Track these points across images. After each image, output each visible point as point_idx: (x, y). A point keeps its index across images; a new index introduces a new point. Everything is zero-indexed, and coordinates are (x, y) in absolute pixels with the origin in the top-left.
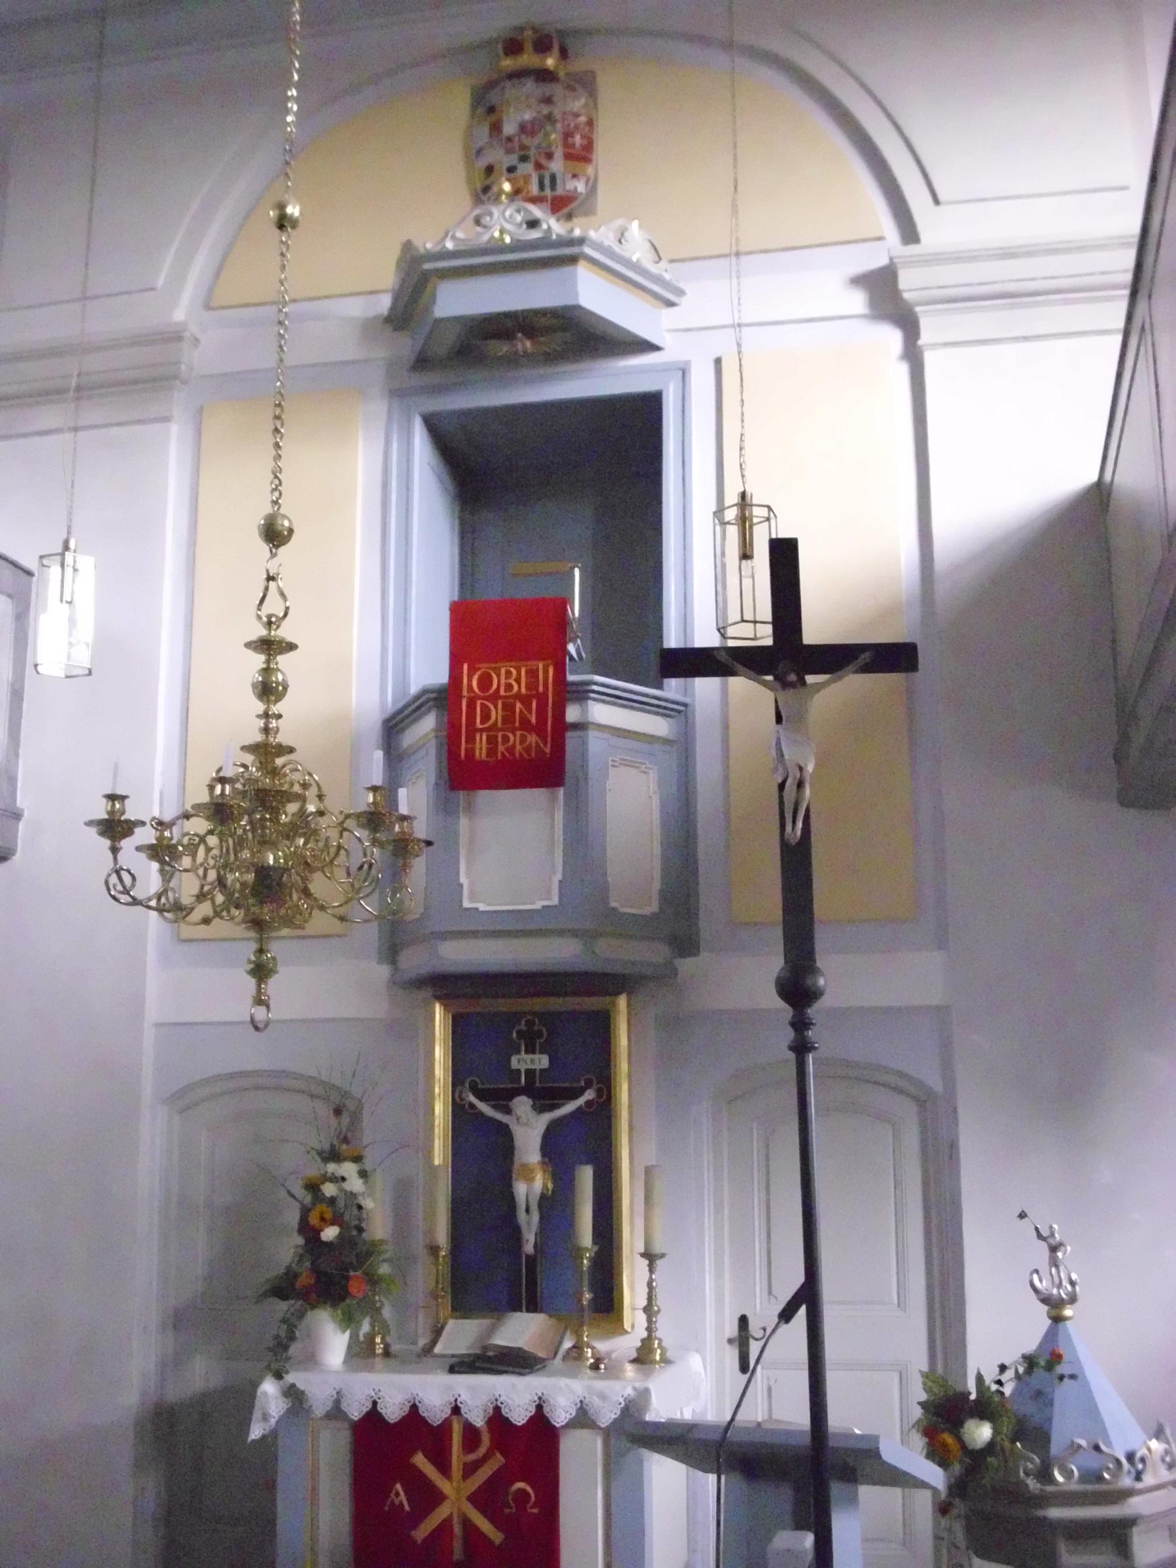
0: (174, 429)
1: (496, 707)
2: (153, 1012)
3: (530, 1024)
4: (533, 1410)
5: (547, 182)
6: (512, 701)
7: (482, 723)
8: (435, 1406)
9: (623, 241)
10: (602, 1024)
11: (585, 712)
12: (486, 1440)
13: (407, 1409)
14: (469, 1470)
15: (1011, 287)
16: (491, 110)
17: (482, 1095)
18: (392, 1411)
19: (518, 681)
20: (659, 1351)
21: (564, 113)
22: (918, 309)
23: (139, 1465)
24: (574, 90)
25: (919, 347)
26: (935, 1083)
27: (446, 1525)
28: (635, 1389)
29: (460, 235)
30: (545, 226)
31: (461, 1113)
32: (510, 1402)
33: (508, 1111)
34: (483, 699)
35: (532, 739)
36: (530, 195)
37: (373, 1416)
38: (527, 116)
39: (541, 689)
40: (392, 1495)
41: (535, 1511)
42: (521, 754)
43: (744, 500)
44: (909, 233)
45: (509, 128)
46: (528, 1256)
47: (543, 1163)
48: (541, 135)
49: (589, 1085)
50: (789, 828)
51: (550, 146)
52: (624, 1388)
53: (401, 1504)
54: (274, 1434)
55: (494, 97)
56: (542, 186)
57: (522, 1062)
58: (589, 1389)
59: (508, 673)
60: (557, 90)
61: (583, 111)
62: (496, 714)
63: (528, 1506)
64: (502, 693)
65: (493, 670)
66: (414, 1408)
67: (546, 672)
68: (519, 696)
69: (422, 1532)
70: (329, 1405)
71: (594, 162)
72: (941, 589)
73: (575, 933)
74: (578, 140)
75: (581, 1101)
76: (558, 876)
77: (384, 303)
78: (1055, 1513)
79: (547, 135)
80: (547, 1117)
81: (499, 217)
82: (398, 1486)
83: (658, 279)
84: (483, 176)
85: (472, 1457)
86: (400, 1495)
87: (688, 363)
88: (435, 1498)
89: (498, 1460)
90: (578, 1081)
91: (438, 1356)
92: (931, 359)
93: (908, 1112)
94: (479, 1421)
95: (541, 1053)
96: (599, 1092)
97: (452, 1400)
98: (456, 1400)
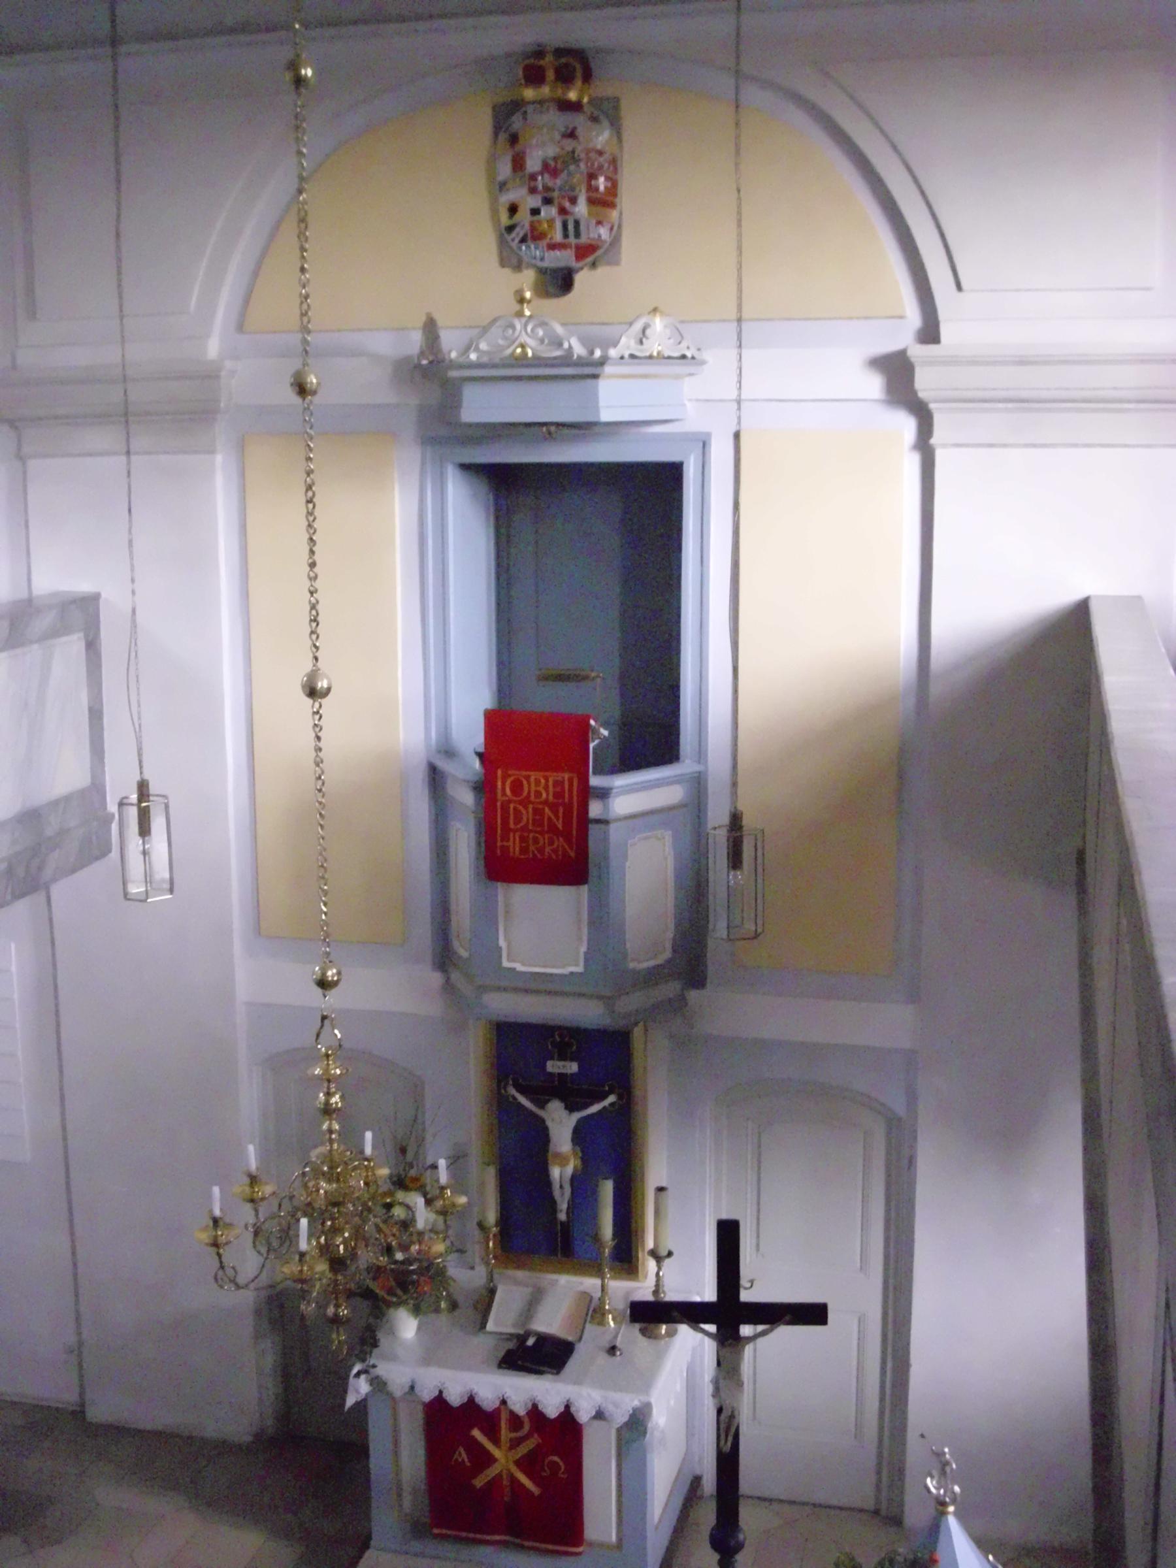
0: (219, 458)
4: (562, 1409)
5: (571, 227)
6: (540, 806)
7: (516, 824)
8: (488, 1398)
9: (644, 340)
11: (606, 808)
12: (527, 1427)
13: (466, 1400)
14: (515, 1444)
15: (1024, 394)
16: (514, 139)
17: (522, 1090)
18: (455, 1397)
19: (546, 788)
22: (932, 406)
23: (258, 1336)
27: (496, 1481)
28: (640, 1400)
29: (483, 346)
30: (566, 345)
34: (515, 802)
35: (560, 842)
36: (553, 241)
38: (551, 151)
39: (567, 795)
43: (736, 821)
45: (533, 164)
46: (562, 1223)
48: (564, 175)
50: (722, 1442)
51: (573, 189)
53: (463, 1461)
54: (365, 1400)
55: (516, 122)
56: (566, 236)
57: (554, 1066)
59: (538, 782)
60: (579, 121)
62: (527, 815)
63: (561, 1472)
64: (532, 798)
65: (520, 804)
68: (546, 802)
69: (479, 1482)
70: (407, 1389)
71: (618, 207)
72: (936, 690)
73: (600, 997)
74: (601, 183)
76: (583, 949)
79: (570, 174)
80: (577, 1116)
81: (521, 331)
82: (462, 1450)
85: (513, 1435)
86: (462, 1455)
87: (709, 435)
88: (490, 1460)
90: (604, 1086)
91: (491, 1333)
92: (941, 457)
94: (520, 1409)
96: (620, 1097)
97: (501, 1395)
98: (503, 1396)
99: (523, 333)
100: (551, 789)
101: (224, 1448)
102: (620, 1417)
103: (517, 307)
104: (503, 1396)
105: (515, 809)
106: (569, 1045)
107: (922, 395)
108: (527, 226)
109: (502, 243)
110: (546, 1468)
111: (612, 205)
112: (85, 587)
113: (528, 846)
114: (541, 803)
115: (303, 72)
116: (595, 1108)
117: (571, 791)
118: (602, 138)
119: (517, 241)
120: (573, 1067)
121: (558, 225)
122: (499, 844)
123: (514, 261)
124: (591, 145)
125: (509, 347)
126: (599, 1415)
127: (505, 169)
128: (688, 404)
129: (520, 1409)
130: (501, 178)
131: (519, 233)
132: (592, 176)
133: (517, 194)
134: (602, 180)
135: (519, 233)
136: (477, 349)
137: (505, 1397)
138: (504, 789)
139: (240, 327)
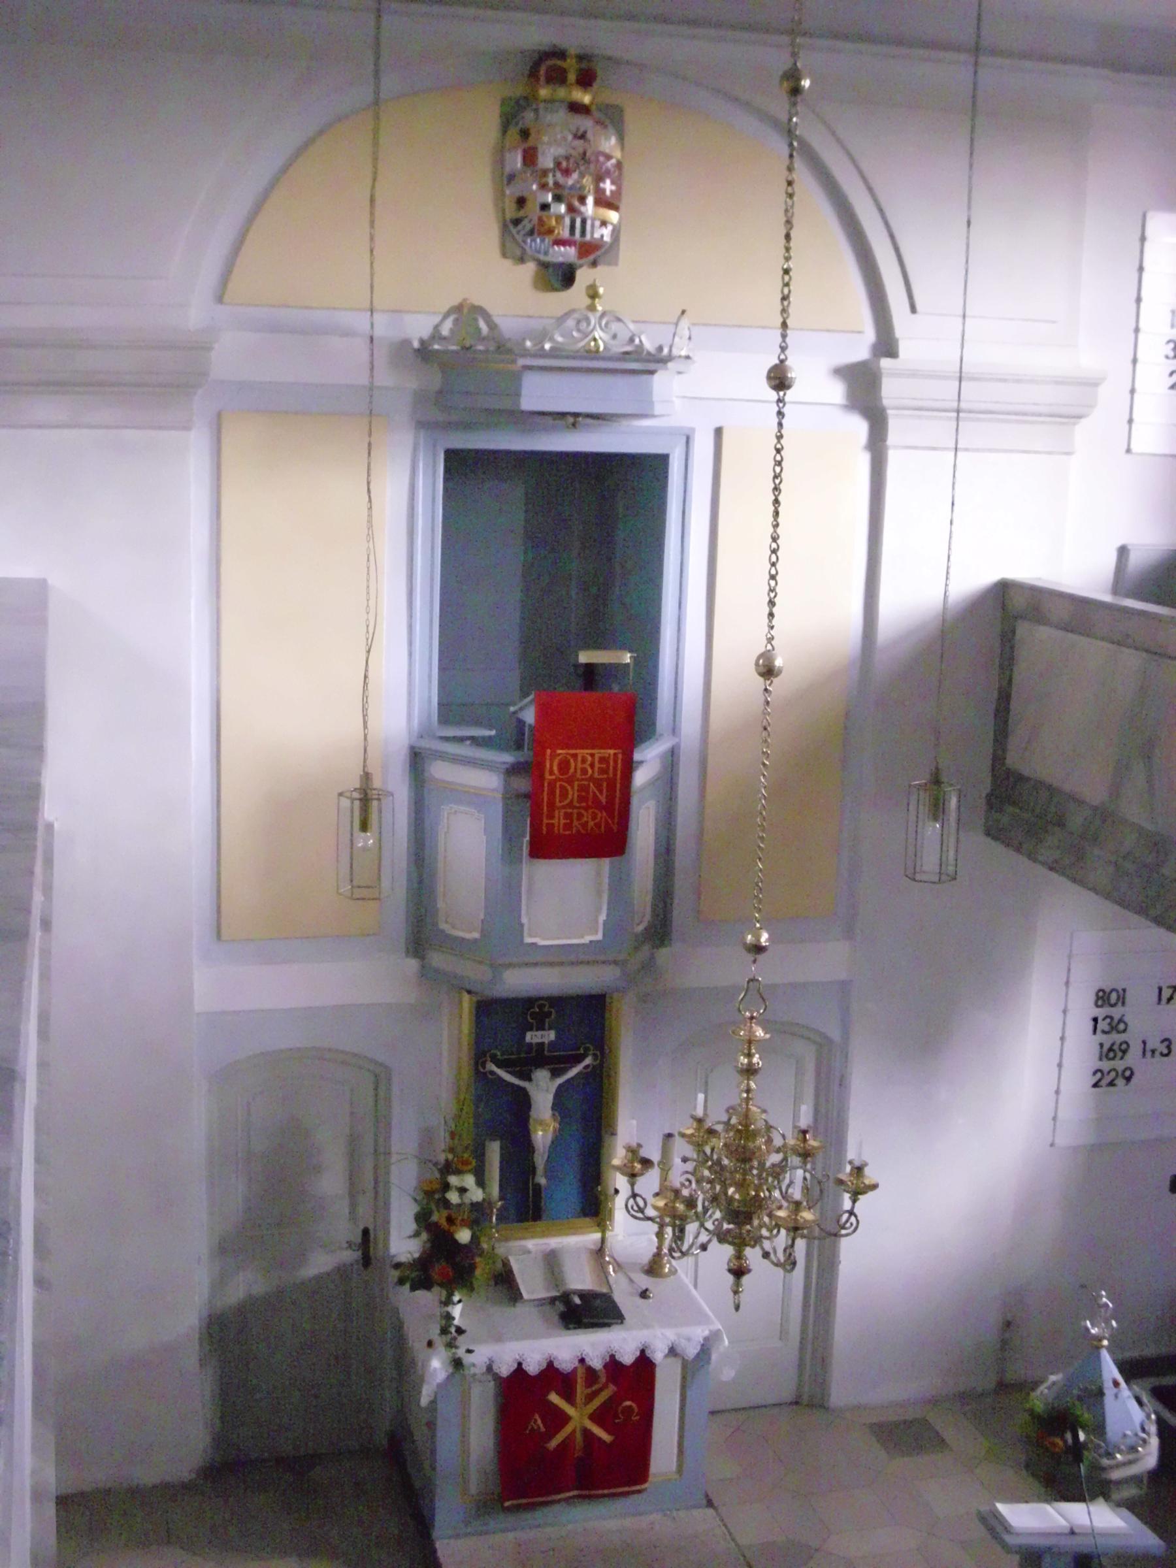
0: (193, 434)
1: (573, 788)
2: (198, 1008)
3: (541, 1007)
4: (638, 1353)
6: (586, 783)
12: (603, 1379)
13: (544, 1365)
14: (590, 1398)
16: (525, 134)
18: (533, 1367)
19: (592, 766)
20: (668, 1266)
22: (890, 412)
24: (606, 127)
25: (886, 446)
26: (835, 1034)
27: (571, 1437)
30: (637, 341)
32: (622, 1351)
33: (530, 1080)
35: (602, 815)
36: (559, 237)
37: (519, 1370)
38: (561, 151)
40: (532, 1423)
41: (638, 1418)
42: (592, 828)
45: (546, 161)
48: (575, 176)
52: (703, 1331)
57: (532, 1037)
58: (679, 1335)
59: (584, 761)
62: (573, 794)
64: (578, 775)
66: (550, 1364)
67: (615, 762)
68: (591, 778)
69: (554, 1444)
76: (603, 917)
78: (1116, 1475)
81: (595, 325)
82: (537, 1417)
84: (514, 206)
85: (589, 1391)
86: (538, 1422)
87: (693, 430)
88: (565, 1419)
89: (612, 1389)
90: (578, 1049)
93: (808, 1054)
94: (597, 1363)
97: (579, 1354)
98: (582, 1354)
99: (597, 326)
100: (597, 765)
101: (171, 1492)
102: (691, 1351)
103: (588, 301)
104: (582, 1354)
105: (561, 786)
106: (549, 1014)
107: (887, 401)
108: (535, 221)
110: (620, 1416)
111: (615, 208)
112: (24, 570)
113: (572, 821)
114: (586, 780)
115: (803, 83)
117: (615, 769)
118: (609, 144)
119: (522, 233)
120: (551, 1035)
121: (567, 221)
122: (545, 821)
123: (518, 252)
125: (582, 339)
126: (672, 1352)
128: (677, 402)
129: (597, 1363)
131: (527, 225)
132: (599, 179)
134: (608, 182)
135: (527, 225)
136: (552, 339)
137: (584, 1353)
138: (552, 767)
139: (220, 299)
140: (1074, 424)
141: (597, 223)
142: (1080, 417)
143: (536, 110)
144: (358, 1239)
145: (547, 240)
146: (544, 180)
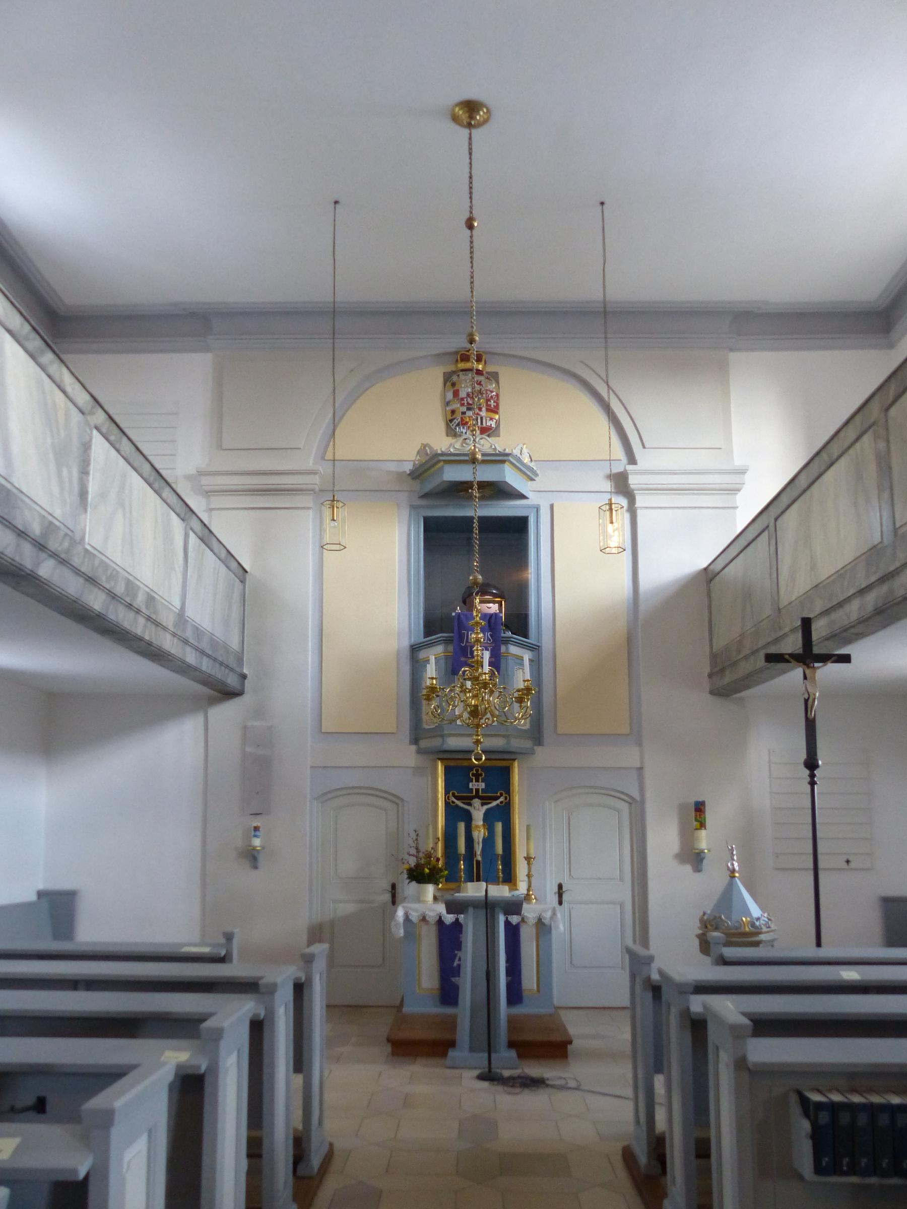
3: (477, 771)
10: (506, 773)
16: (453, 385)
17: (458, 798)
21: (486, 390)
22: (635, 492)
26: (636, 795)
31: (447, 804)
33: (470, 804)
44: (632, 460)
45: (462, 394)
47: (484, 825)
49: (501, 795)
51: (480, 405)
55: (455, 378)
57: (473, 785)
61: (494, 390)
72: (643, 607)
75: (498, 802)
77: (408, 467)
80: (485, 807)
83: (531, 469)
90: (497, 793)
92: (640, 514)
93: (625, 807)
95: (482, 782)
96: (506, 798)
106: (481, 775)
109: (448, 426)
111: (497, 413)
116: (494, 803)
119: (455, 425)
124: (487, 388)
127: (450, 396)
130: (447, 400)
132: (488, 400)
133: (456, 405)
134: (492, 402)
140: (736, 494)
141: (488, 419)
142: (739, 490)
143: (458, 376)
144: (390, 889)
145: (465, 428)
146: (462, 402)
